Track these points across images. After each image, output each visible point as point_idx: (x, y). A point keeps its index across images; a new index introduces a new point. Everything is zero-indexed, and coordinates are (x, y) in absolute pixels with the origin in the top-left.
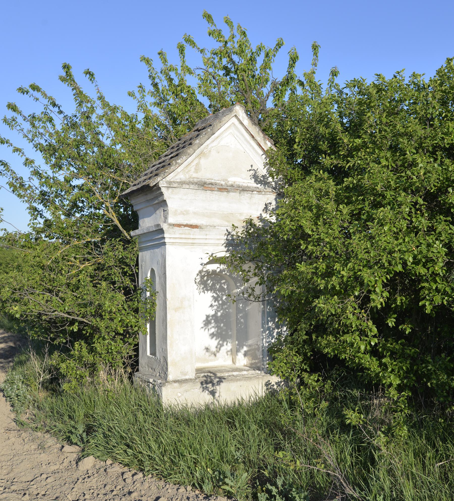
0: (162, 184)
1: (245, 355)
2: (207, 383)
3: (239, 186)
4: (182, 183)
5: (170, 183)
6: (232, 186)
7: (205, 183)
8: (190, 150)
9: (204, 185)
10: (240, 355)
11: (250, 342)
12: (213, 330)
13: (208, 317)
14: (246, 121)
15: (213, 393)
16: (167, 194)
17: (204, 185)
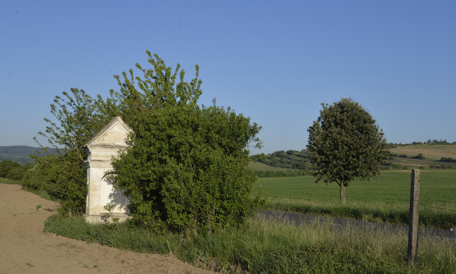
0: (89, 147)
1: (124, 209)
2: (103, 217)
3: (119, 146)
4: (96, 146)
5: (91, 146)
6: (116, 146)
7: (106, 145)
8: (99, 134)
9: (104, 146)
10: (122, 209)
11: (126, 204)
12: (113, 199)
13: (111, 194)
14: (122, 122)
15: (105, 221)
16: (90, 150)
17: (104, 146)
